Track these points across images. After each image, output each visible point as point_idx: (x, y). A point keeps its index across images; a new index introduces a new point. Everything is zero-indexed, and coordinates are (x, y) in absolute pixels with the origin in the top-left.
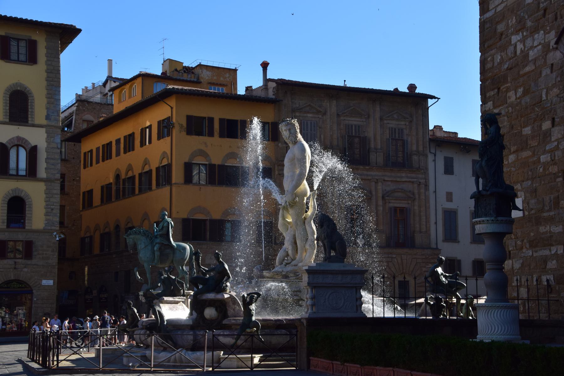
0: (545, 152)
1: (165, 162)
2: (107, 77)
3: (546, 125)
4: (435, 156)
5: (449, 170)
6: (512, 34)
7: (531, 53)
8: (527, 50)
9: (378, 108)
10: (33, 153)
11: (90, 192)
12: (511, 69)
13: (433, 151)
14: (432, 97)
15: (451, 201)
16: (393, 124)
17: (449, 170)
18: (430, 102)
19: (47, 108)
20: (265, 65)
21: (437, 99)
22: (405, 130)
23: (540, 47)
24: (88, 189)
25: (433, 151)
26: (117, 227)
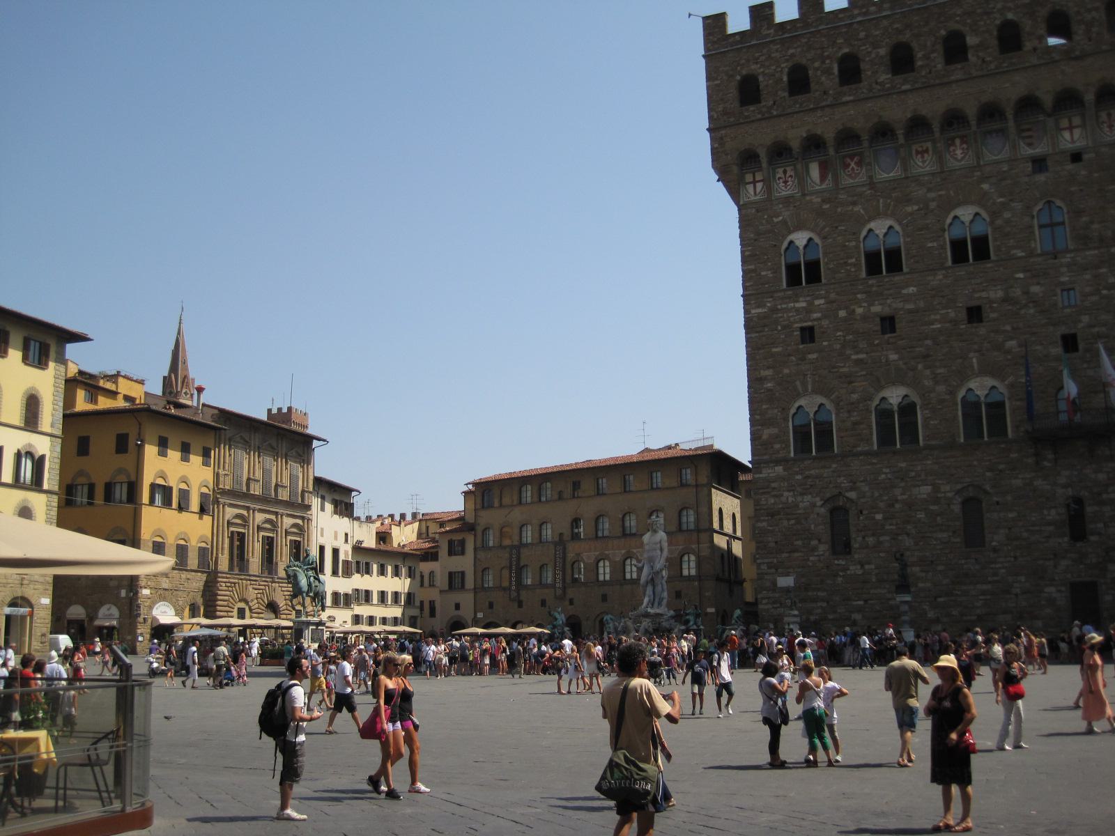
0: (811, 556)
3: (814, 542)
6: (784, 491)
7: (801, 504)
9: (284, 445)
10: (39, 464)
12: (784, 509)
14: (319, 439)
17: (323, 509)
19: (53, 415)
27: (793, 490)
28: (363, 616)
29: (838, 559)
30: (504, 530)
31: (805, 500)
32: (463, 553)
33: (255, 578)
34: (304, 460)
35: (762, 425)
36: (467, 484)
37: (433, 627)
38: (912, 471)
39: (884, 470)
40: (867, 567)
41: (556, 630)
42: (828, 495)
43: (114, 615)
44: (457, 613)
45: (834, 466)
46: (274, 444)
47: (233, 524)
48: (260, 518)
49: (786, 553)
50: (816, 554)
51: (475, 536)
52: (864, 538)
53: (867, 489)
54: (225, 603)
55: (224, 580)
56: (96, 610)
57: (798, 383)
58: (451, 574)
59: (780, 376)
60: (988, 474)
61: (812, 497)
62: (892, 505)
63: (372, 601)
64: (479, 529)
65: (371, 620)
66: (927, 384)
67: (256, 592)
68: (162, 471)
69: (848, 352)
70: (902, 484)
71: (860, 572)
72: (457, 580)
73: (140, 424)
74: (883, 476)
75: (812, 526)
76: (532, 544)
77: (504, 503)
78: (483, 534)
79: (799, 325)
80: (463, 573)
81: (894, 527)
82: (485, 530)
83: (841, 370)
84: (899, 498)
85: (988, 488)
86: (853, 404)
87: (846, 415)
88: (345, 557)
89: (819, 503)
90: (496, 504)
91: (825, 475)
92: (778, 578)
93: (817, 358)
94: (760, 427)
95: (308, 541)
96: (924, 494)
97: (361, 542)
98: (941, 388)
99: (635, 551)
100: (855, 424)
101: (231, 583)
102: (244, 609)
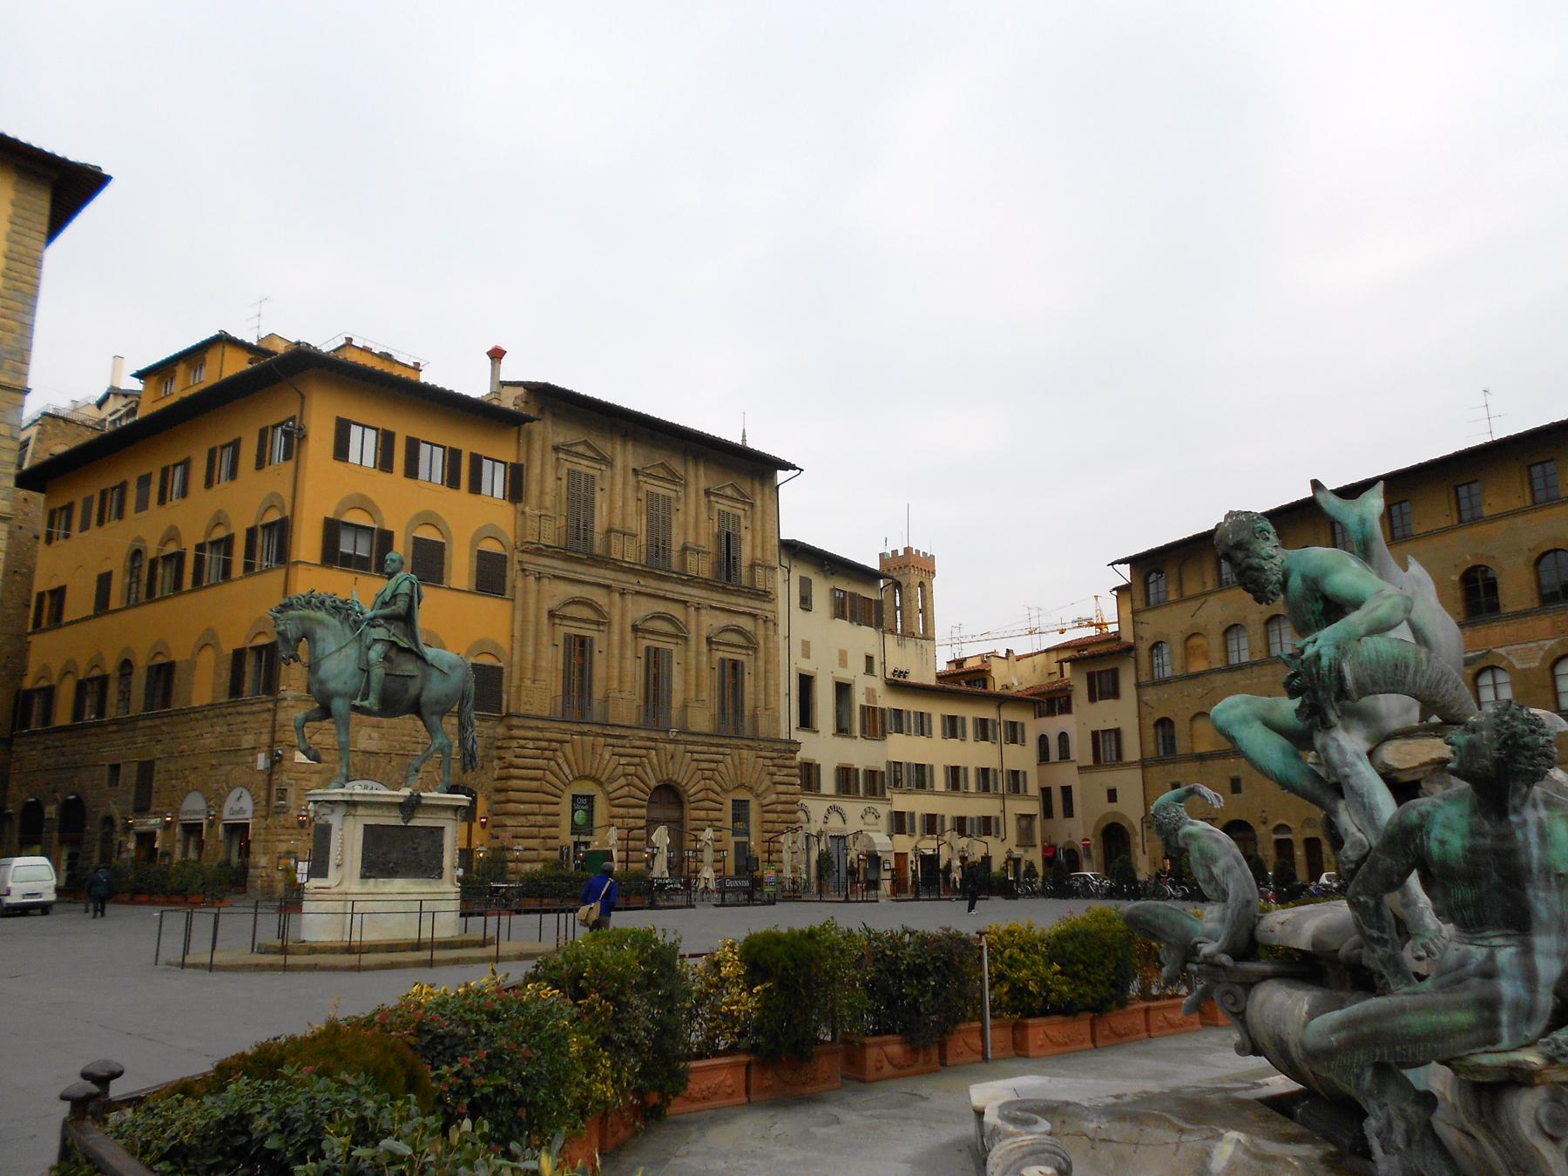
1: (273, 516)
2: (109, 389)
4: (789, 572)
5: (806, 603)
9: (702, 472)
11: (59, 594)
13: (785, 562)
14: (787, 466)
15: (809, 658)
16: (724, 505)
17: (806, 603)
18: (781, 475)
20: (496, 355)
21: (798, 471)
22: (742, 519)
24: (54, 585)
25: (787, 565)
26: (126, 666)
28: (912, 815)
30: (1195, 641)
32: (1115, 694)
33: (617, 732)
34: (752, 505)
36: (1112, 564)
37: (1070, 836)
41: (1349, 743)
43: (244, 812)
44: (1113, 807)
46: (680, 471)
47: (565, 617)
48: (639, 609)
51: (1136, 660)
54: (534, 784)
55: (531, 734)
56: (222, 799)
58: (1095, 735)
63: (932, 786)
64: (1143, 649)
65: (931, 823)
67: (623, 761)
68: (363, 497)
72: (1108, 747)
73: (303, 397)
76: (1252, 664)
77: (1188, 591)
78: (1151, 656)
80: (1117, 732)
82: (1156, 646)
88: (868, 701)
90: (1173, 597)
95: (766, 663)
97: (905, 674)
99: (1502, 651)
101: (550, 741)
102: (575, 797)
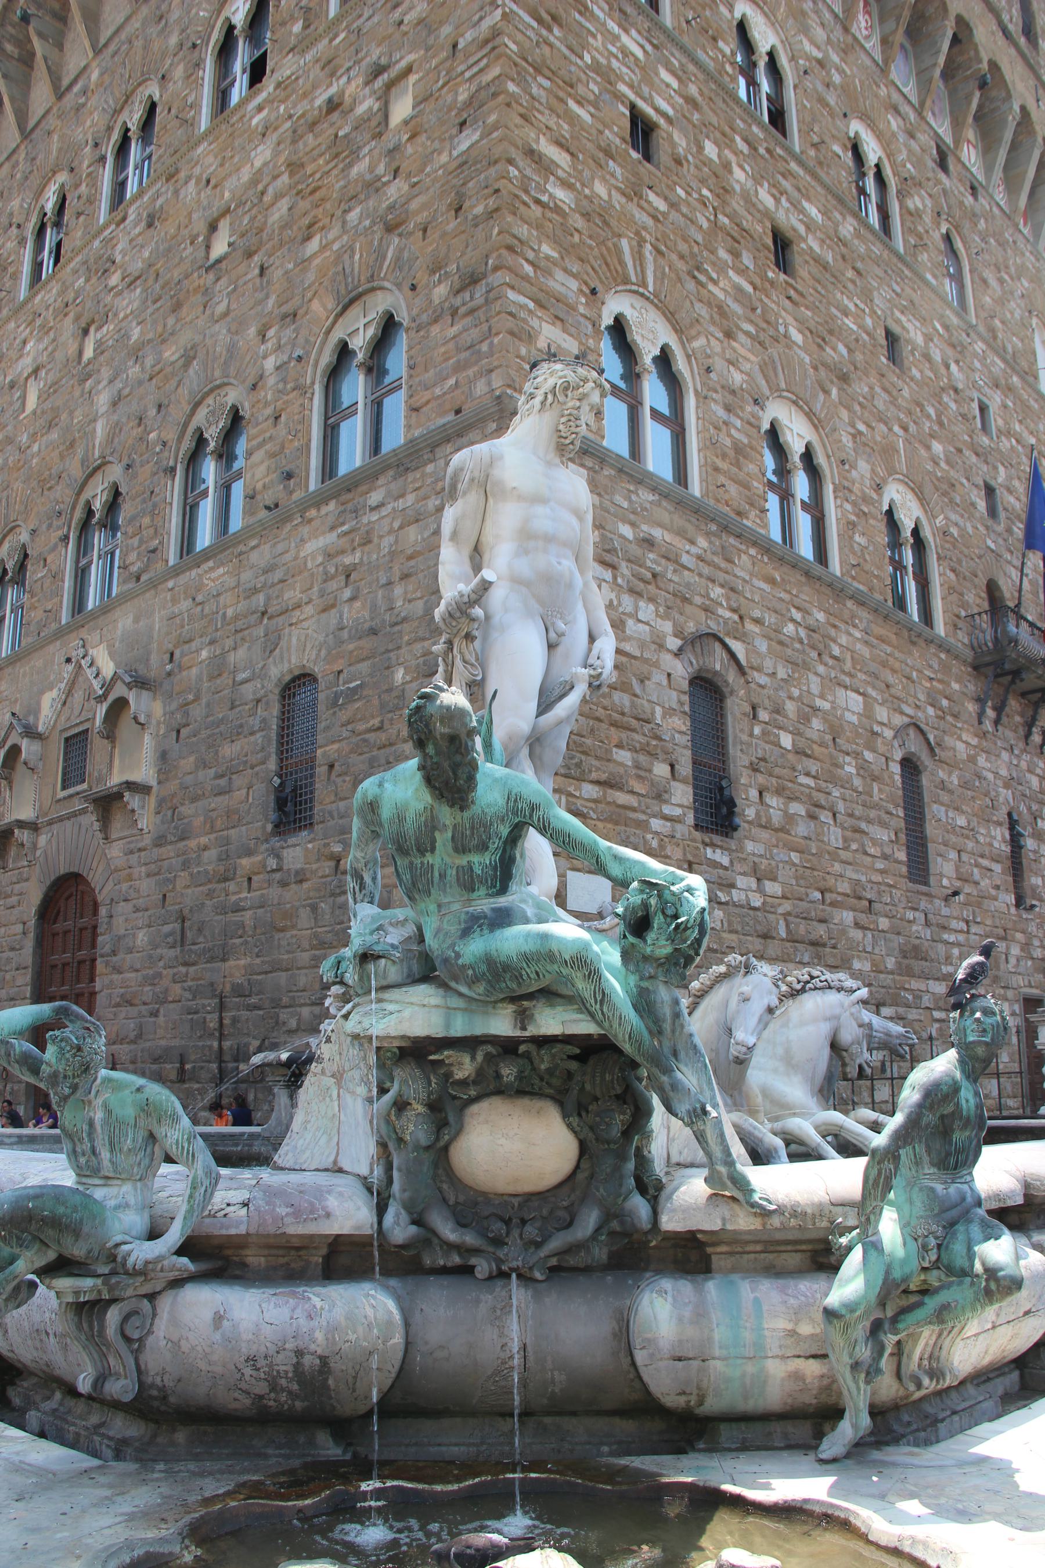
7: (630, 622)
8: (623, 613)
23: (647, 628)
27: (613, 567)
29: (712, 845)
31: (641, 616)
35: (536, 302)
38: (834, 641)
39: (793, 611)
40: (773, 888)
42: (691, 627)
45: (702, 542)
49: (598, 783)
50: (667, 810)
52: (761, 793)
53: (763, 646)
57: (624, 243)
59: (587, 191)
60: (931, 711)
61: (657, 615)
62: (805, 719)
66: (844, 440)
69: (723, 254)
70: (821, 669)
71: (757, 902)
74: (790, 629)
75: (658, 710)
79: (632, 96)
81: (811, 782)
83: (711, 287)
84: (819, 703)
85: (931, 738)
86: (733, 392)
87: (721, 412)
89: (673, 643)
91: (685, 559)
92: (570, 874)
93: (663, 214)
94: (531, 305)
96: (853, 713)
98: (863, 466)
100: (739, 449)
